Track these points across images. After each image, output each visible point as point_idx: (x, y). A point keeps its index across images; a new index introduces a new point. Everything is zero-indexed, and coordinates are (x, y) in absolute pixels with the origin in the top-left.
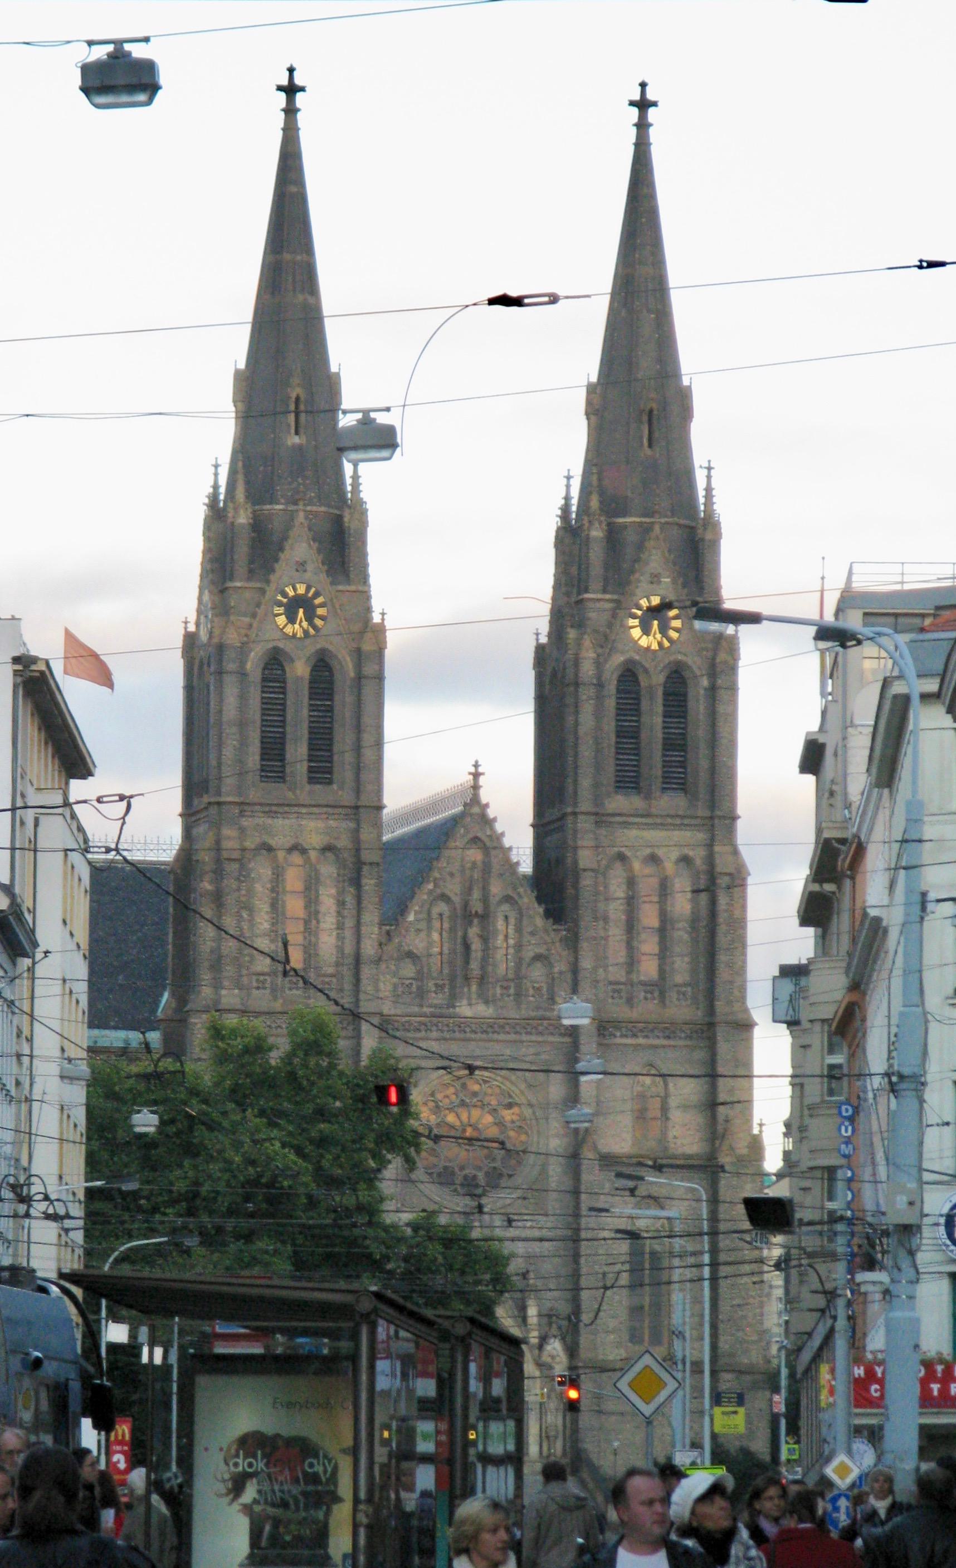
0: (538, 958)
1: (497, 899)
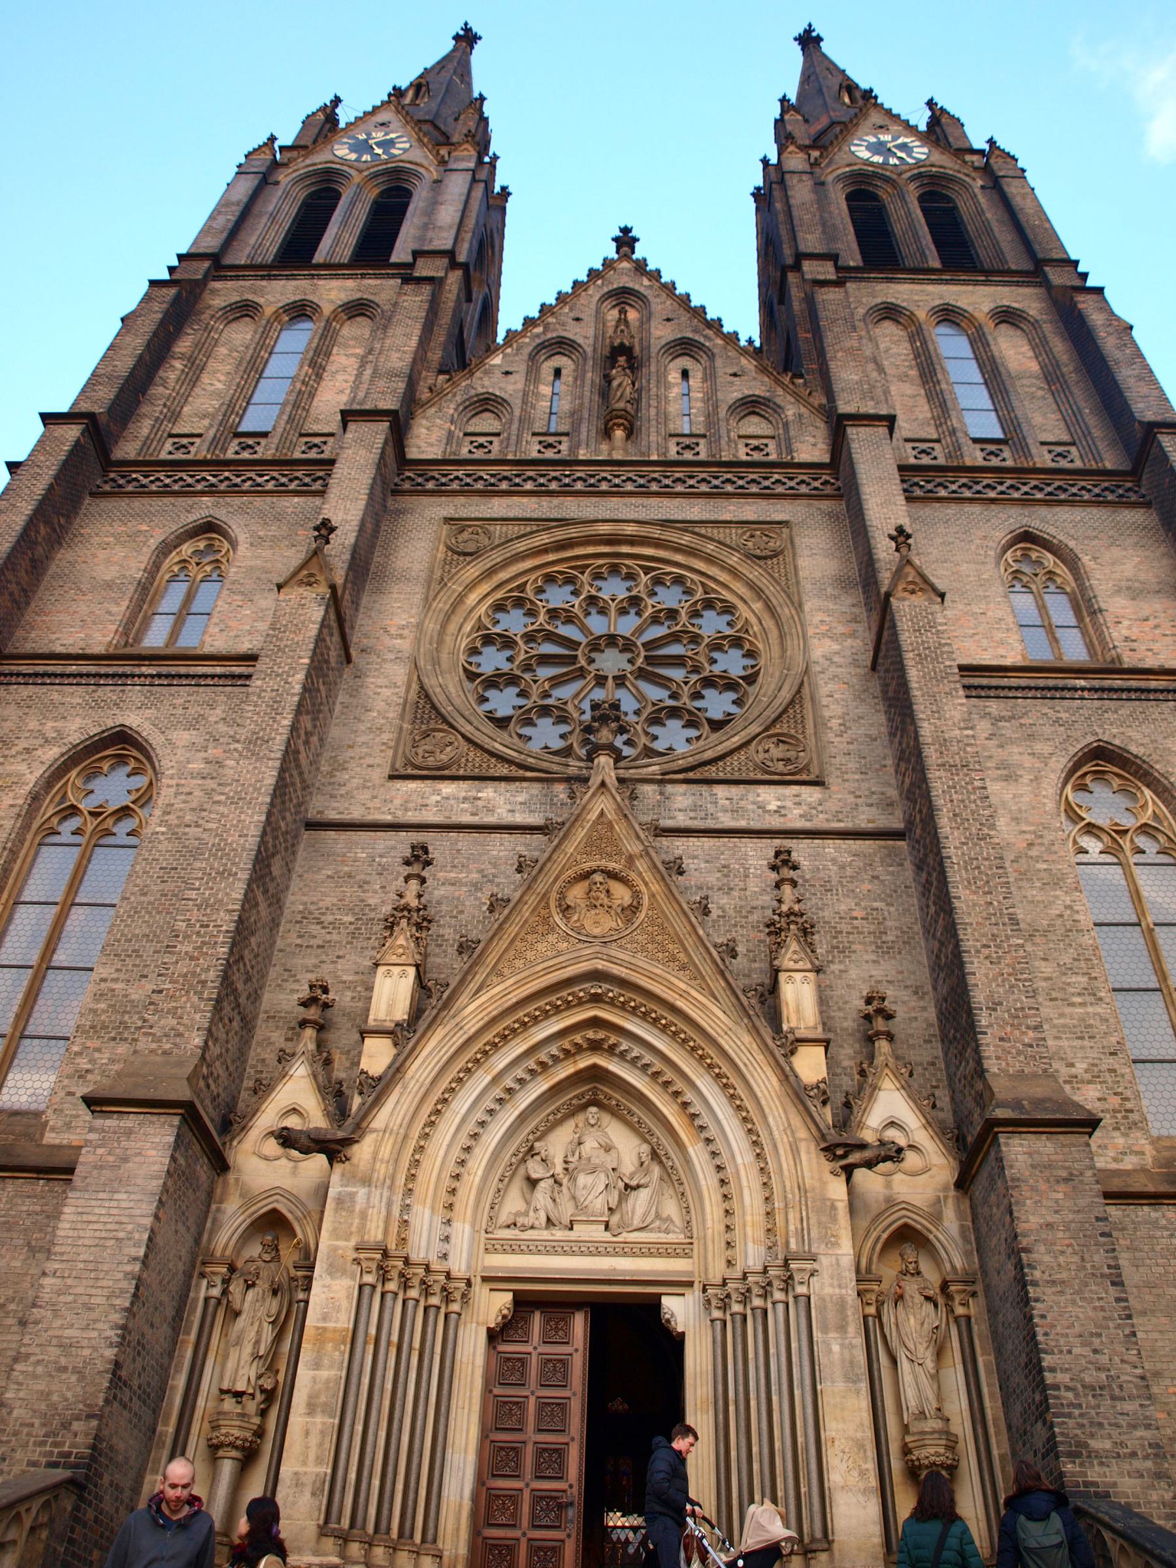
0: (751, 406)
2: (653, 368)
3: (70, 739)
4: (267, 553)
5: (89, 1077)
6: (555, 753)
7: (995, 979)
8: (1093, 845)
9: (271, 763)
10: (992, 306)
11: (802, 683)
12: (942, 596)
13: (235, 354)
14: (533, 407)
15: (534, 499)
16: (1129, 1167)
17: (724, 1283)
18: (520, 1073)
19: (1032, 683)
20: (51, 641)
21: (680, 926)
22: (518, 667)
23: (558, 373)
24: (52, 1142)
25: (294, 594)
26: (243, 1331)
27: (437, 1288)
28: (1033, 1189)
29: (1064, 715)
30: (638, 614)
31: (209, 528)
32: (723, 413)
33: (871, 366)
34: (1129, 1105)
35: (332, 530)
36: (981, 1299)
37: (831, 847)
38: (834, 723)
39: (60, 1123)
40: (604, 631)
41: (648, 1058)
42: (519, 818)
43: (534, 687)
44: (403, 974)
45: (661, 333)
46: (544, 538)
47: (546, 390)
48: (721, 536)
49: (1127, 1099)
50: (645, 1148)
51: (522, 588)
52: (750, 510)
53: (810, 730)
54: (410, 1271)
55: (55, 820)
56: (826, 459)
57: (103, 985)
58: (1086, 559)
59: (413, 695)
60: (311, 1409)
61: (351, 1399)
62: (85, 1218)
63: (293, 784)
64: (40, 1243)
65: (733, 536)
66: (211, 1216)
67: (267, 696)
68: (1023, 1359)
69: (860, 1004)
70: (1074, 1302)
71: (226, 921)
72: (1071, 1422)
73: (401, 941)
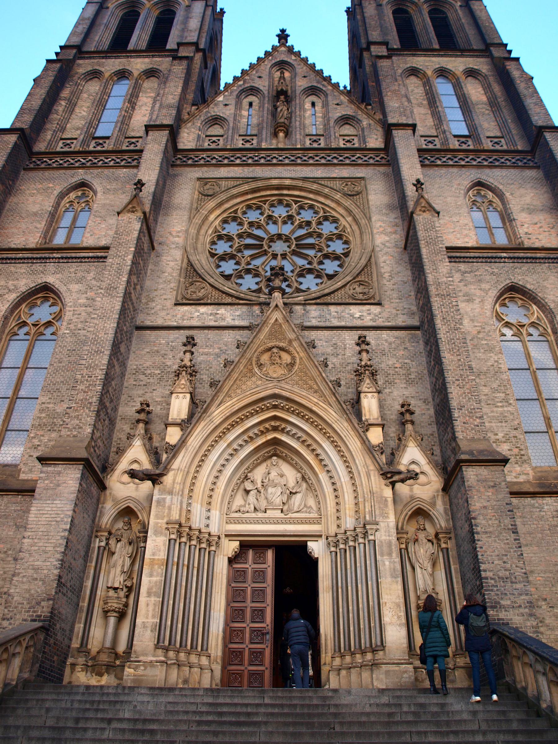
0: (345, 120)
1: (302, 88)
2: (298, 102)
3: (21, 289)
4: (111, 197)
5: (39, 448)
6: (253, 291)
7: (461, 395)
8: (508, 332)
9: (118, 299)
10: (464, 68)
11: (371, 256)
12: (438, 213)
13: (91, 97)
14: (239, 122)
15: (241, 168)
16: (522, 480)
17: (336, 535)
18: (240, 442)
19: (481, 255)
20: (9, 242)
21: (314, 372)
22: (235, 250)
23: (251, 104)
24: (24, 478)
25: (126, 216)
26: (116, 561)
27: (204, 540)
28: (478, 491)
29: (496, 270)
30: (292, 224)
31: (83, 185)
32: (332, 123)
33: (404, 99)
34: (522, 452)
35: (143, 185)
36: (453, 540)
37: (385, 334)
38: (386, 275)
39: (27, 470)
40: (276, 232)
41: (300, 434)
42: (237, 323)
43: (243, 260)
44: (184, 397)
45: (302, 84)
46: (246, 187)
47: (245, 113)
48: (332, 185)
49: (522, 450)
50: (299, 475)
51: (236, 212)
52: (345, 172)
53: (375, 278)
54: (192, 533)
55: (16, 328)
56: (382, 146)
57: (43, 405)
58: (507, 195)
59: (185, 265)
60: (149, 594)
61: (167, 590)
62: (41, 512)
63: (129, 309)
64: (21, 524)
65: (337, 185)
66: (99, 510)
67: (115, 266)
68: (472, 566)
69: (399, 407)
70: (495, 541)
71: (100, 374)
72: (493, 593)
73: (183, 382)
